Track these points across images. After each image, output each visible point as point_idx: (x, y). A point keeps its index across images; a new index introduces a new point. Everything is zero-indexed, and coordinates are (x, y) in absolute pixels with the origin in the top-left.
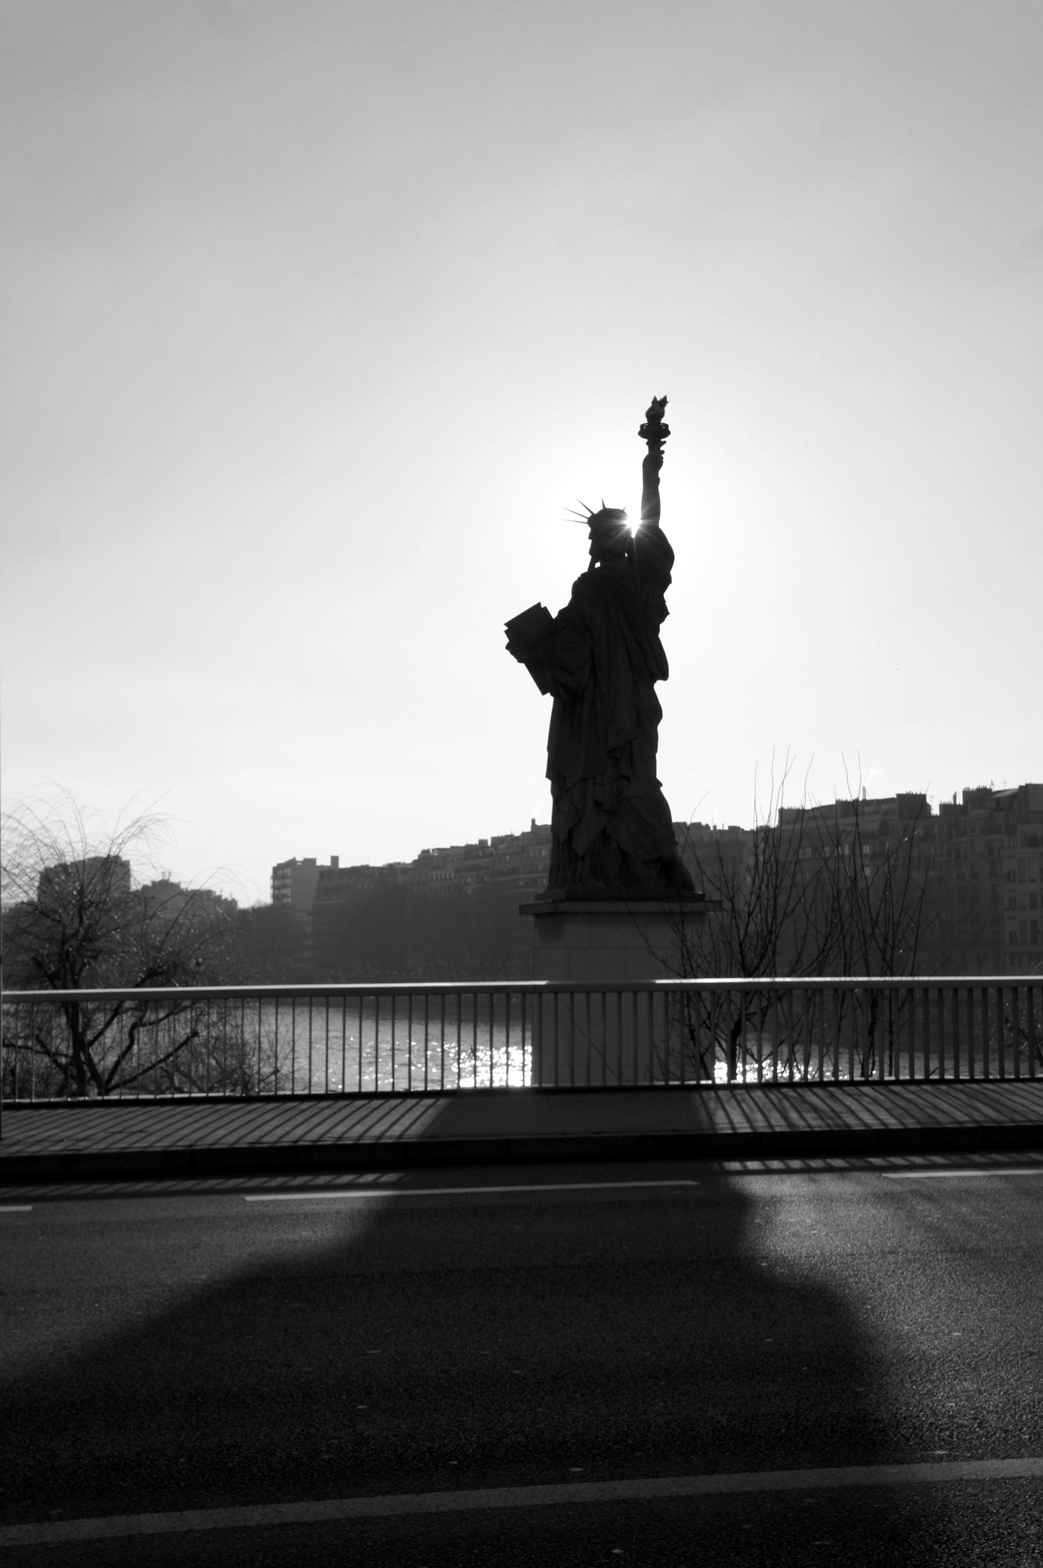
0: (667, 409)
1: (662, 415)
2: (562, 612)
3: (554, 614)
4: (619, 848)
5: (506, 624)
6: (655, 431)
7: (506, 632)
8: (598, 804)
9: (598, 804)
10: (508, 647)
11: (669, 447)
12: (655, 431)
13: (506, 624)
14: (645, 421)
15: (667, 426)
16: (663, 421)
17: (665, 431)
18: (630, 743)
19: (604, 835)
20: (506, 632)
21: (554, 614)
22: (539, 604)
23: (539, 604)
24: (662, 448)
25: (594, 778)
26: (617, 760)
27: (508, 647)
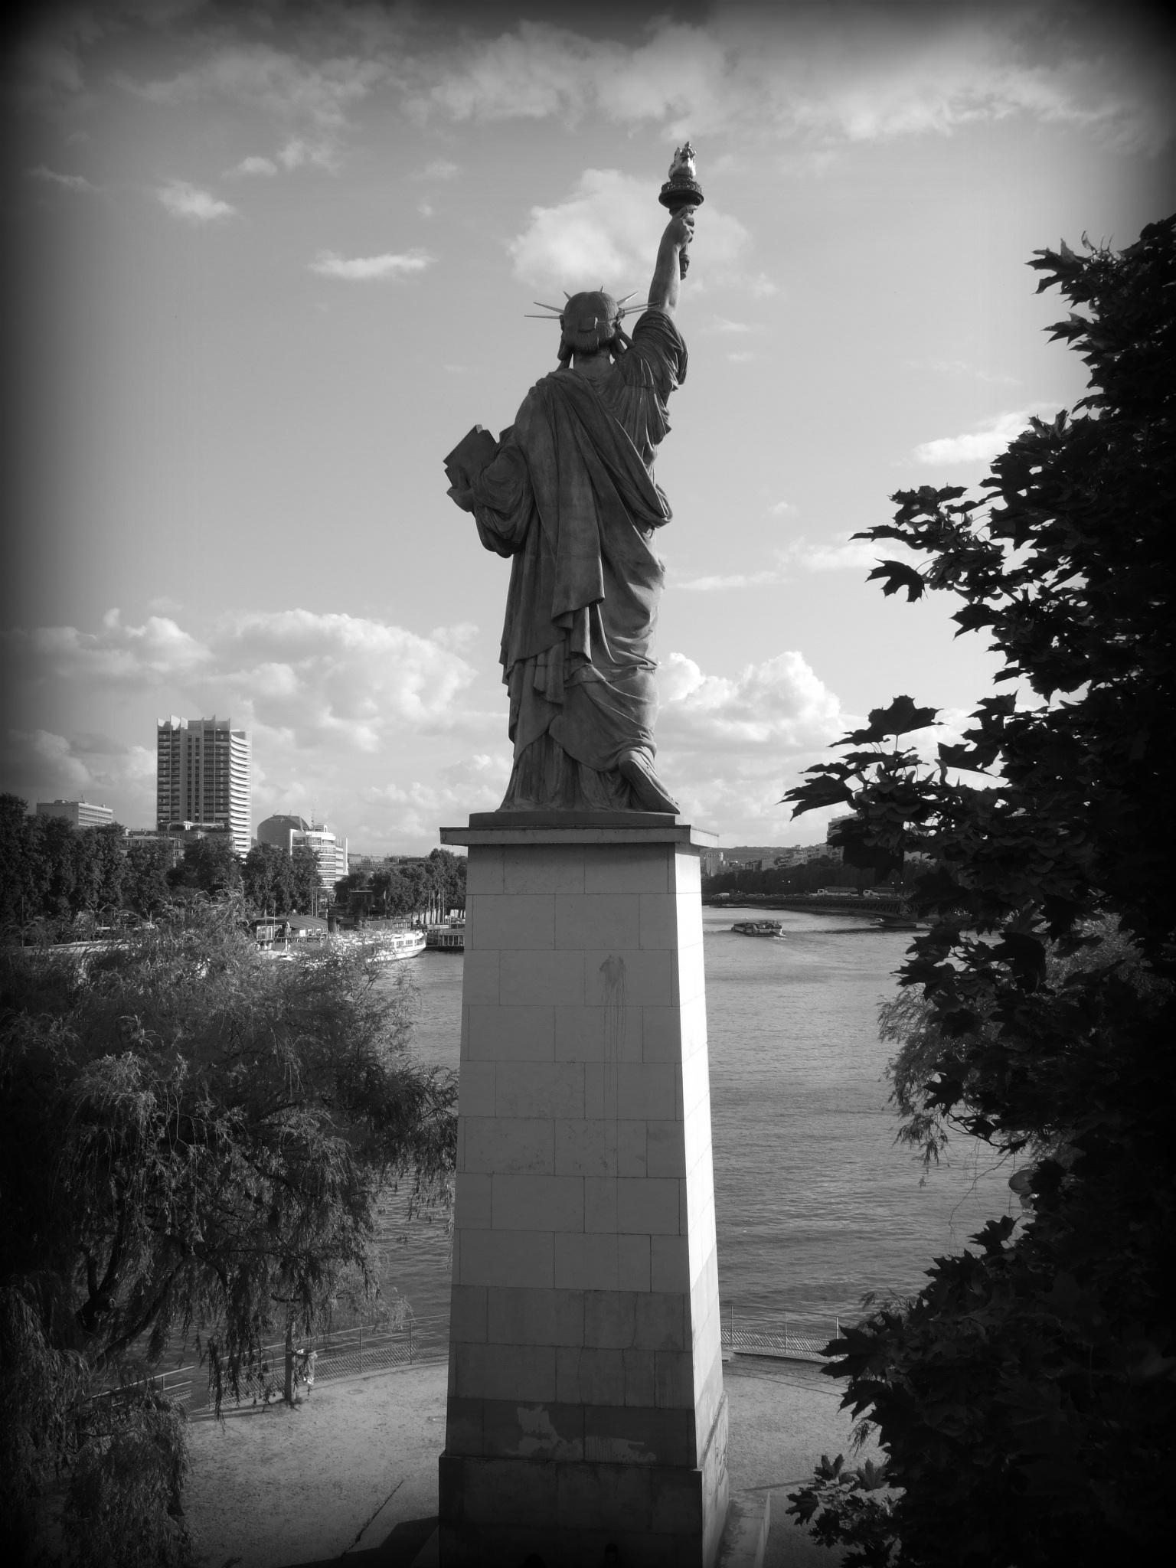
2: (504, 434)
3: (497, 440)
5: (446, 461)
8: (538, 694)
9: (538, 694)
10: (449, 493)
11: (699, 215)
12: (680, 195)
13: (446, 461)
19: (546, 738)
21: (497, 440)
26: (568, 632)
27: (449, 493)
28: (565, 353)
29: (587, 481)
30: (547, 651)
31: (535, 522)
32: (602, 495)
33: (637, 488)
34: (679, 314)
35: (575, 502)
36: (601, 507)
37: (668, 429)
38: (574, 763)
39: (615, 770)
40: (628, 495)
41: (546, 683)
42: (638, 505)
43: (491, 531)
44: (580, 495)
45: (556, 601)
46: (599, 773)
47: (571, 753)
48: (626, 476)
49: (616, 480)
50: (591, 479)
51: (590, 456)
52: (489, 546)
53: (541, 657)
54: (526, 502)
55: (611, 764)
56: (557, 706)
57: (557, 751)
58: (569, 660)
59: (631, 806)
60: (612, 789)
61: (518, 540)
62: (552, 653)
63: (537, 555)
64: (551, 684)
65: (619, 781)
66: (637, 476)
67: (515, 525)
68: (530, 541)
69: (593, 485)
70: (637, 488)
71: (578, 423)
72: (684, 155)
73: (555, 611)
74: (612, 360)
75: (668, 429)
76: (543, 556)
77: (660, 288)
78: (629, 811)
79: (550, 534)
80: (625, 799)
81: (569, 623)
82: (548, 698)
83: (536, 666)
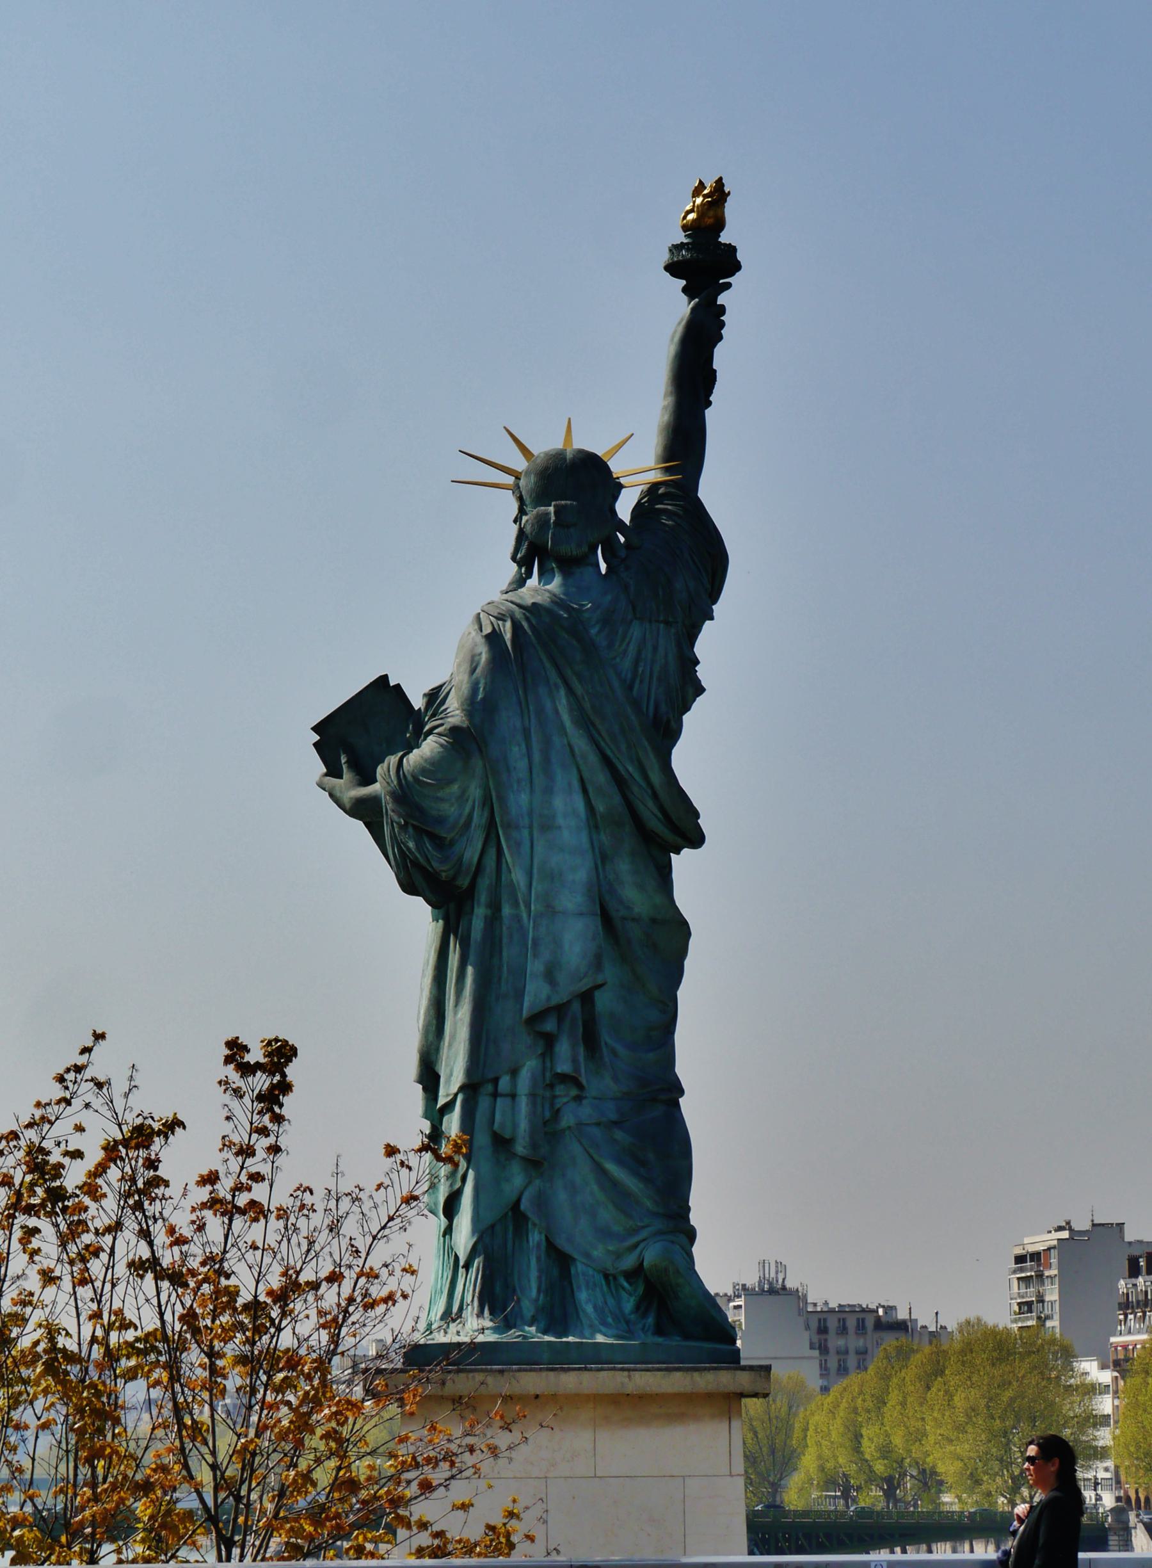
0: (730, 209)
1: (720, 224)
4: (551, 1246)
5: (316, 729)
6: (704, 262)
7: (316, 745)
11: (737, 299)
12: (704, 262)
13: (316, 729)
14: (681, 237)
15: (731, 250)
16: (724, 238)
17: (727, 262)
18: (587, 998)
20: (316, 745)
21: (418, 703)
22: (384, 679)
23: (384, 679)
24: (721, 300)
25: (496, 1081)
26: (549, 1041)
28: (531, 552)
29: (576, 784)
30: (514, 1072)
31: (492, 853)
32: (600, 808)
33: (655, 796)
34: (713, 492)
35: (560, 821)
36: (597, 827)
37: (700, 690)
38: (560, 1261)
39: (636, 1273)
40: (641, 808)
41: (515, 1126)
42: (655, 824)
43: (416, 864)
44: (567, 806)
45: (531, 987)
46: (606, 1277)
47: (561, 1243)
48: (637, 776)
49: (620, 781)
50: (582, 780)
51: (581, 743)
52: (409, 888)
53: (504, 1083)
54: (479, 819)
55: (629, 1262)
56: (534, 1164)
57: (535, 1237)
58: (551, 1086)
59: (659, 1331)
60: (629, 1304)
61: (464, 882)
62: (525, 1075)
63: (495, 907)
64: (523, 1125)
65: (641, 1289)
66: (656, 778)
67: (460, 860)
68: (484, 883)
69: (585, 791)
70: (655, 796)
71: (562, 692)
72: (719, 194)
73: (528, 1005)
74: (603, 567)
75: (700, 690)
76: (506, 910)
77: (685, 442)
78: (660, 1340)
79: (518, 876)
80: (650, 1320)
81: (550, 1026)
82: (520, 1148)
83: (495, 1095)
